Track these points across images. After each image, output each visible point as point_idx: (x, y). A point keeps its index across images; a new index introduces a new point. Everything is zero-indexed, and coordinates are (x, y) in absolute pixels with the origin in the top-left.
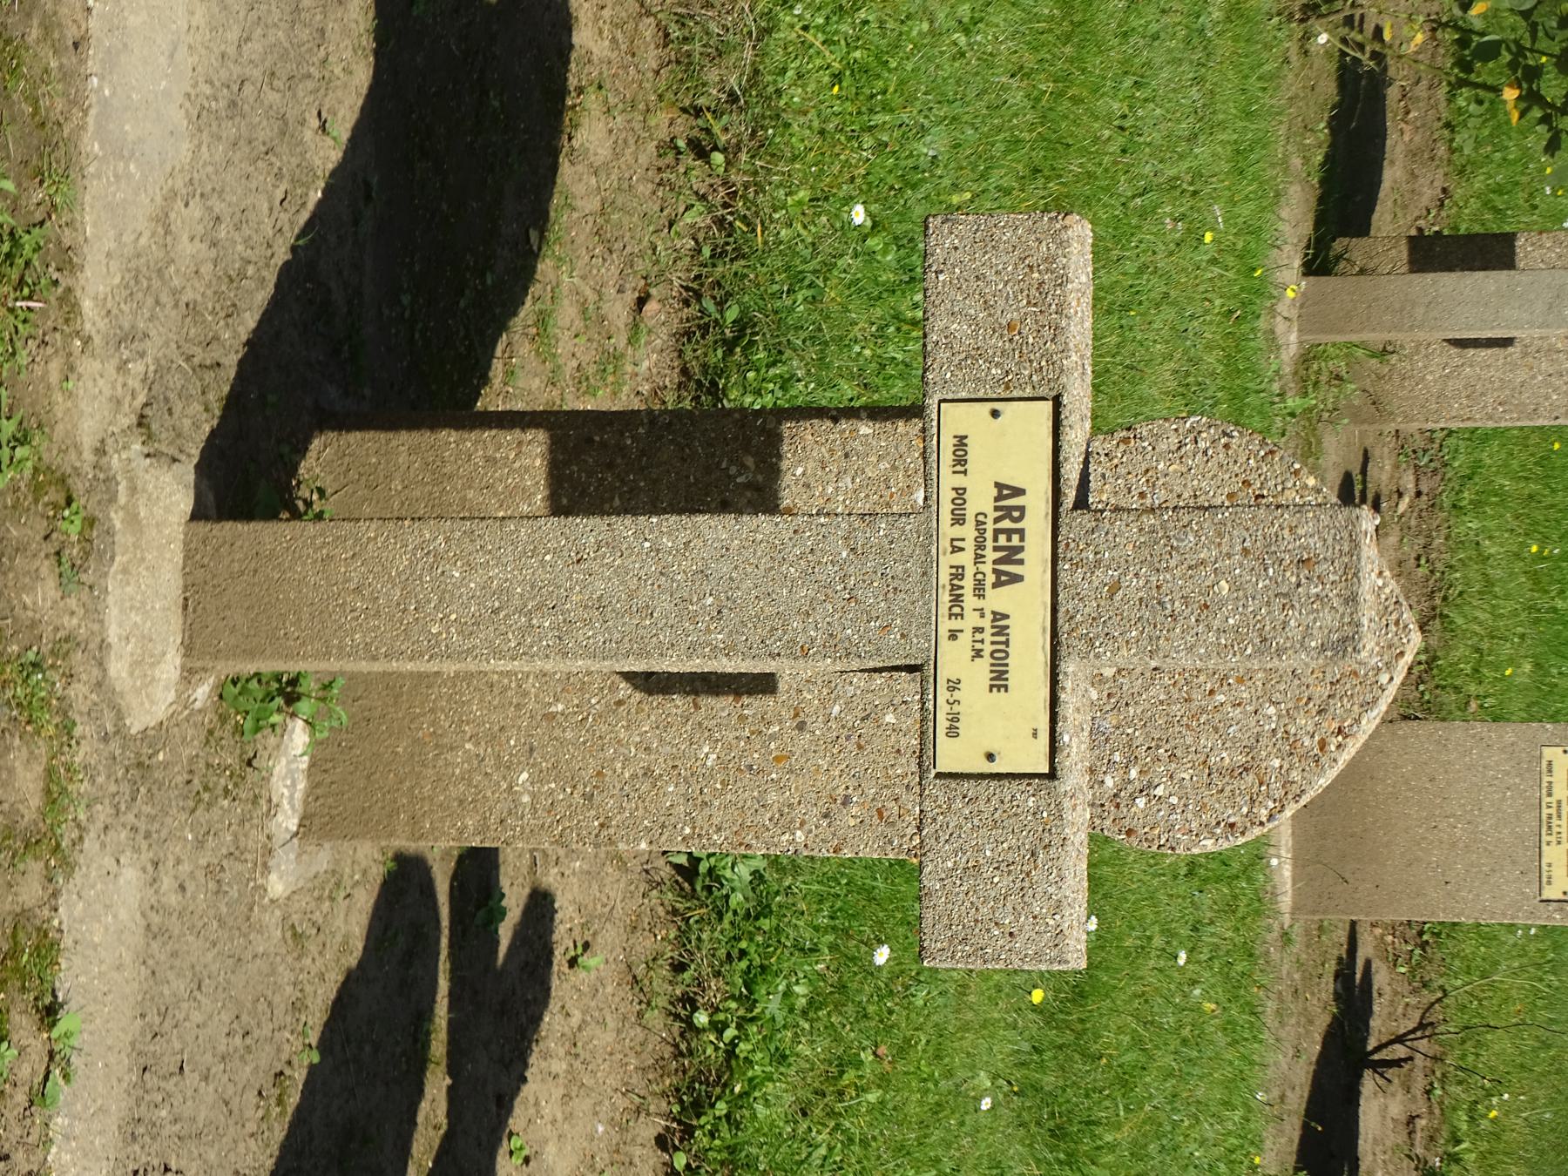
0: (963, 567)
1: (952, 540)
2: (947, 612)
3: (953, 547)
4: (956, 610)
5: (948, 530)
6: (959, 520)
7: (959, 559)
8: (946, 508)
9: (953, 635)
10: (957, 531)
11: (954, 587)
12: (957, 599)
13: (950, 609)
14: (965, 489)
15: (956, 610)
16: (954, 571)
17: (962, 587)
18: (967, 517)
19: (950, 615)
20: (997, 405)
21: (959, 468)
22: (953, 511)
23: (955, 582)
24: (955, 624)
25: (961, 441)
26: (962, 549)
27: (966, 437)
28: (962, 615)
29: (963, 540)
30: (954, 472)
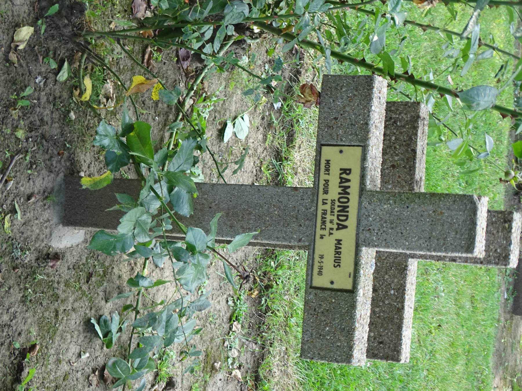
0: (326, 210)
1: (323, 200)
2: (320, 227)
3: (323, 202)
4: (323, 227)
5: (321, 196)
6: (326, 192)
8: (321, 187)
9: (322, 237)
10: (325, 196)
11: (323, 218)
12: (324, 222)
13: (321, 226)
15: (323, 227)
16: (323, 212)
17: (326, 218)
18: (329, 192)
19: (321, 228)
21: (327, 172)
23: (323, 216)
24: (323, 232)
25: (328, 162)
26: (326, 203)
27: (330, 160)
28: (325, 229)
29: (327, 200)
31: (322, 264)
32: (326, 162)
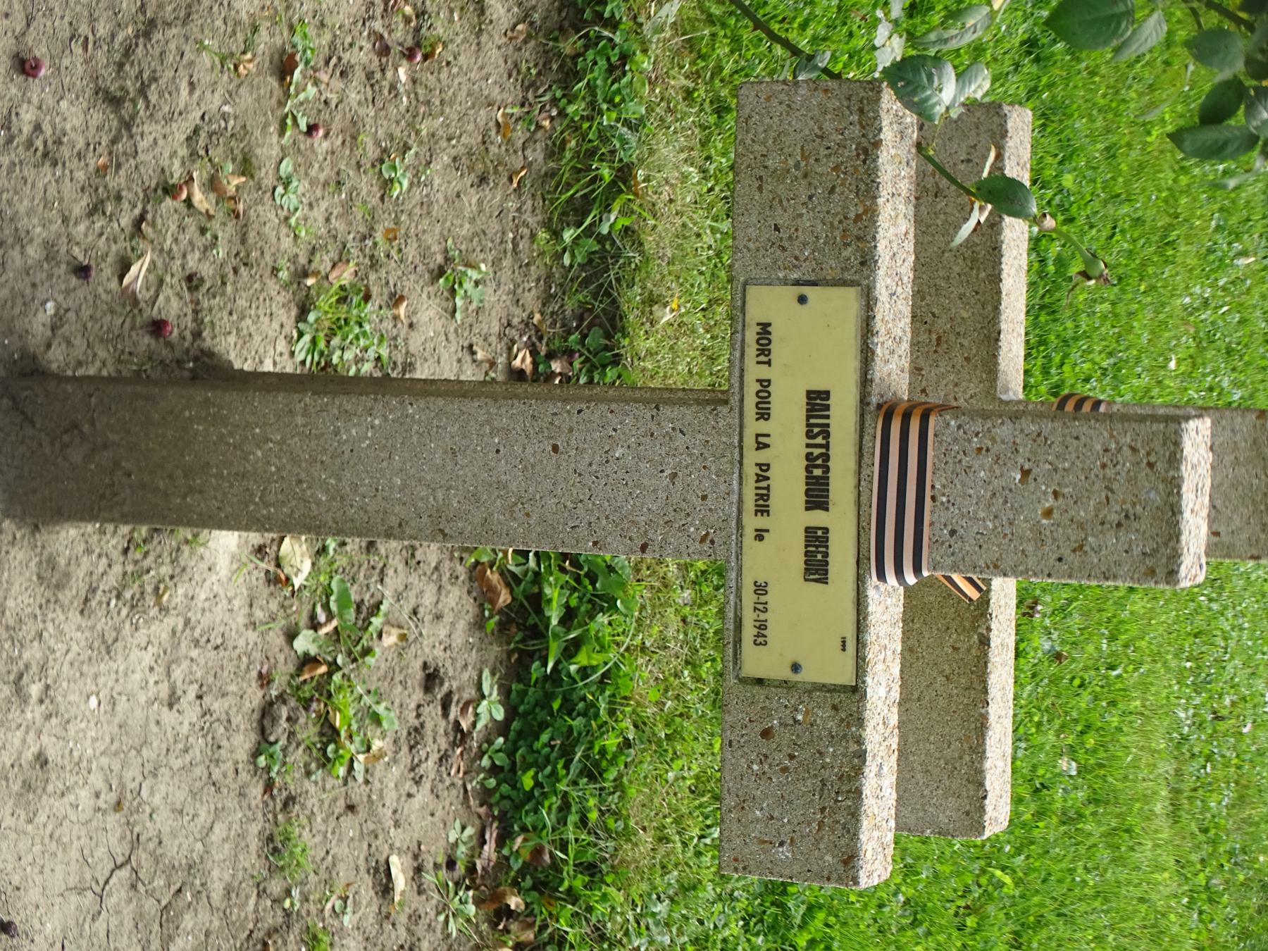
1: (758, 436)
3: (758, 443)
5: (753, 427)
6: (764, 415)
7: (763, 456)
10: (763, 427)
14: (769, 381)
18: (772, 412)
20: (806, 290)
21: (763, 358)
22: (758, 403)
25: (765, 328)
26: (767, 446)
27: (769, 325)
29: (768, 436)
30: (758, 363)
31: (763, 616)
32: (758, 329)
